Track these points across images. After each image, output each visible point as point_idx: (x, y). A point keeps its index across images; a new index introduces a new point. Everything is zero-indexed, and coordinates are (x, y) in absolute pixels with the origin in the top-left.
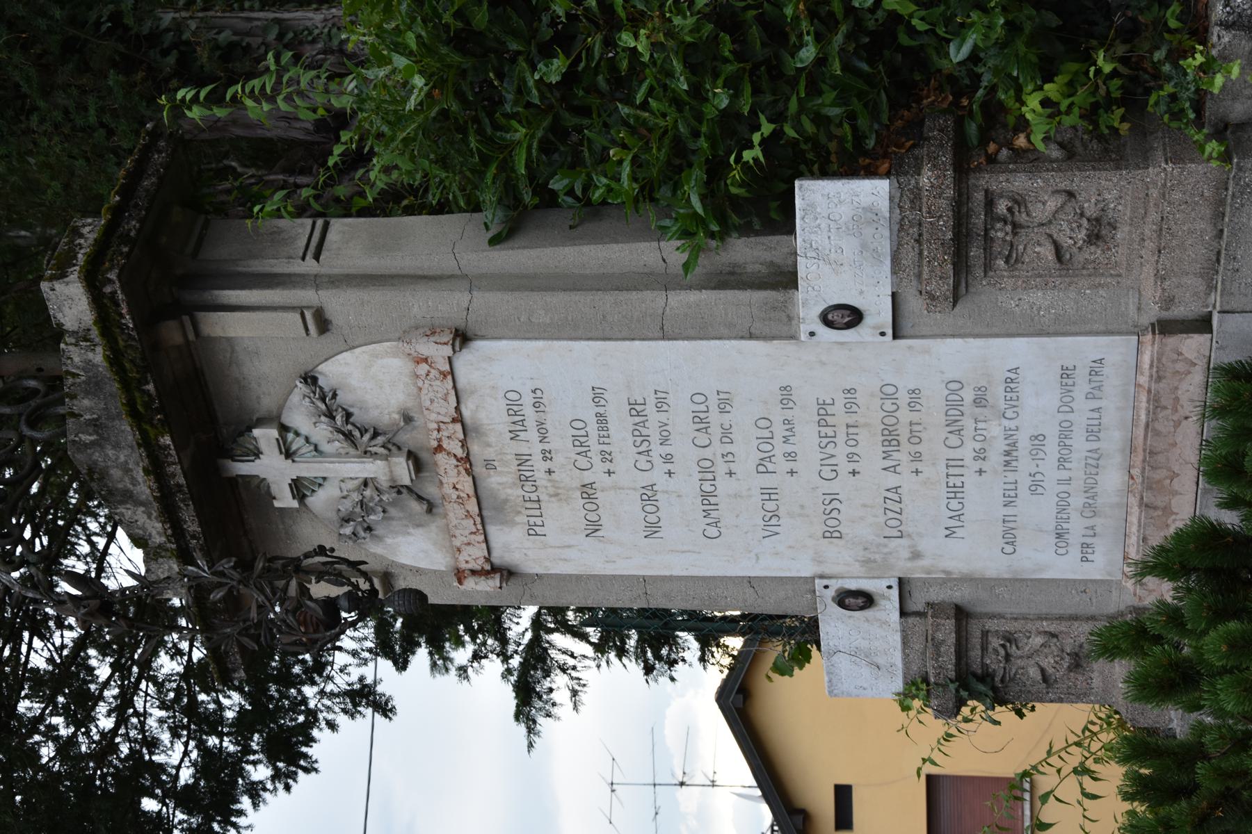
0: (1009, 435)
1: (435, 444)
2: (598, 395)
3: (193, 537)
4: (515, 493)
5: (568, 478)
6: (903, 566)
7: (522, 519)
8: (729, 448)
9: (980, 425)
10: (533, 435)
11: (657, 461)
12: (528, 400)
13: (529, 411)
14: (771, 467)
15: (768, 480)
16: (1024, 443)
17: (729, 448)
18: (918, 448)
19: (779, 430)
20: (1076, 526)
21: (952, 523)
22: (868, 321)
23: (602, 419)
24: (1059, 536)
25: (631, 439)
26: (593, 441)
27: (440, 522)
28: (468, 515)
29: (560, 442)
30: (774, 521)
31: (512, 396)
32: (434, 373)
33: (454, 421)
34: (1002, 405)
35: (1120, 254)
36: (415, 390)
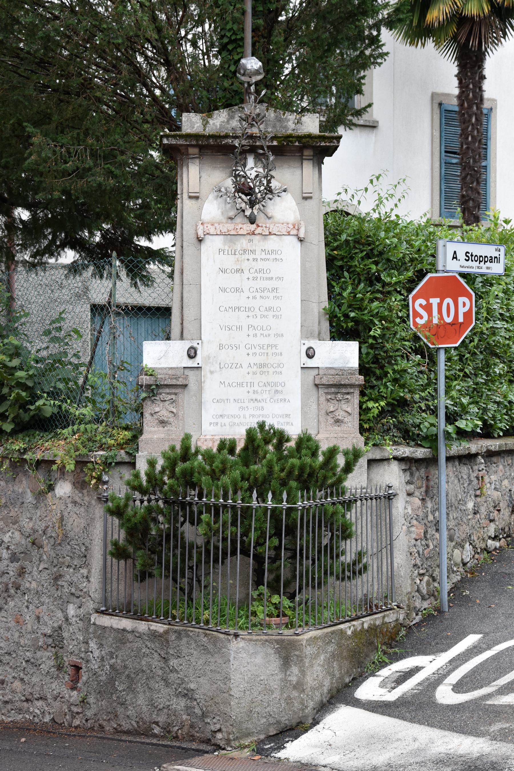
0: (264, 400)
1: (260, 225)
2: (279, 278)
3: (232, 141)
4: (238, 247)
5: (245, 266)
6: (206, 370)
7: (227, 248)
8: (259, 317)
9: (267, 392)
10: (263, 256)
11: (254, 294)
12: (278, 257)
13: (273, 256)
14: (251, 329)
15: (245, 328)
16: (260, 405)
17: (259, 317)
18: (258, 374)
19: (266, 333)
20: (226, 421)
21: (226, 384)
22: (309, 360)
23: (271, 279)
24: (221, 416)
25: (263, 287)
26: (261, 275)
27: (224, 221)
28: (228, 231)
29: (260, 265)
30: (227, 328)
31: (279, 252)
32: (289, 230)
33: (270, 233)
34: (275, 398)
35: (330, 428)
36: (282, 222)
